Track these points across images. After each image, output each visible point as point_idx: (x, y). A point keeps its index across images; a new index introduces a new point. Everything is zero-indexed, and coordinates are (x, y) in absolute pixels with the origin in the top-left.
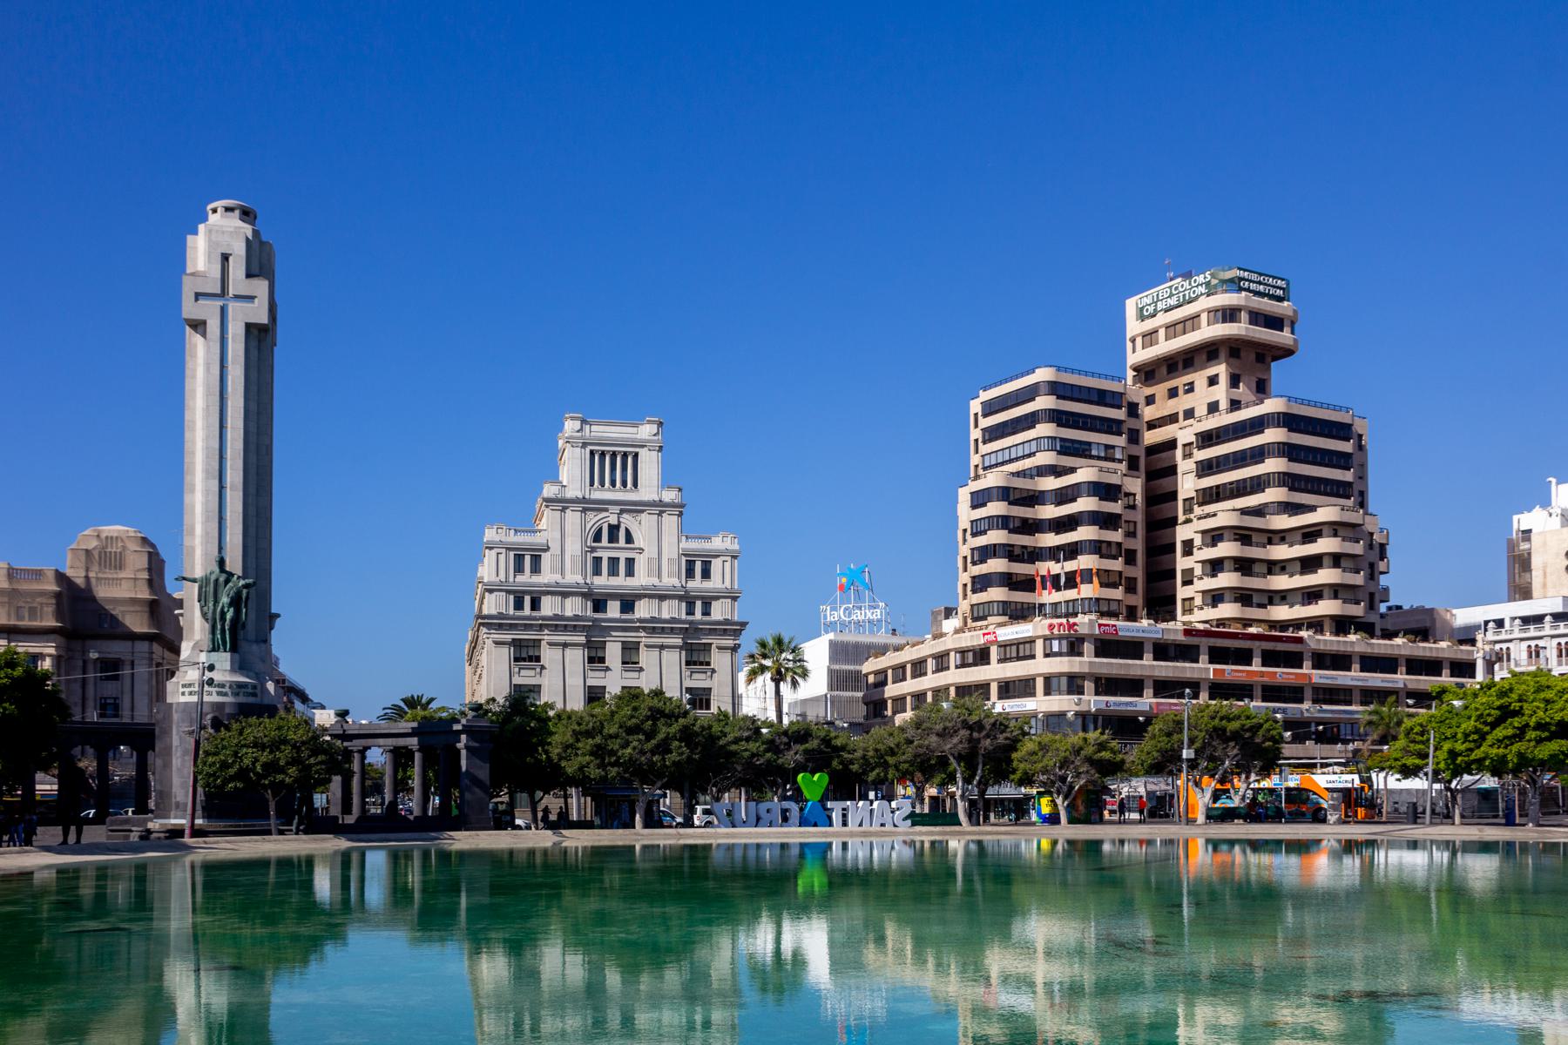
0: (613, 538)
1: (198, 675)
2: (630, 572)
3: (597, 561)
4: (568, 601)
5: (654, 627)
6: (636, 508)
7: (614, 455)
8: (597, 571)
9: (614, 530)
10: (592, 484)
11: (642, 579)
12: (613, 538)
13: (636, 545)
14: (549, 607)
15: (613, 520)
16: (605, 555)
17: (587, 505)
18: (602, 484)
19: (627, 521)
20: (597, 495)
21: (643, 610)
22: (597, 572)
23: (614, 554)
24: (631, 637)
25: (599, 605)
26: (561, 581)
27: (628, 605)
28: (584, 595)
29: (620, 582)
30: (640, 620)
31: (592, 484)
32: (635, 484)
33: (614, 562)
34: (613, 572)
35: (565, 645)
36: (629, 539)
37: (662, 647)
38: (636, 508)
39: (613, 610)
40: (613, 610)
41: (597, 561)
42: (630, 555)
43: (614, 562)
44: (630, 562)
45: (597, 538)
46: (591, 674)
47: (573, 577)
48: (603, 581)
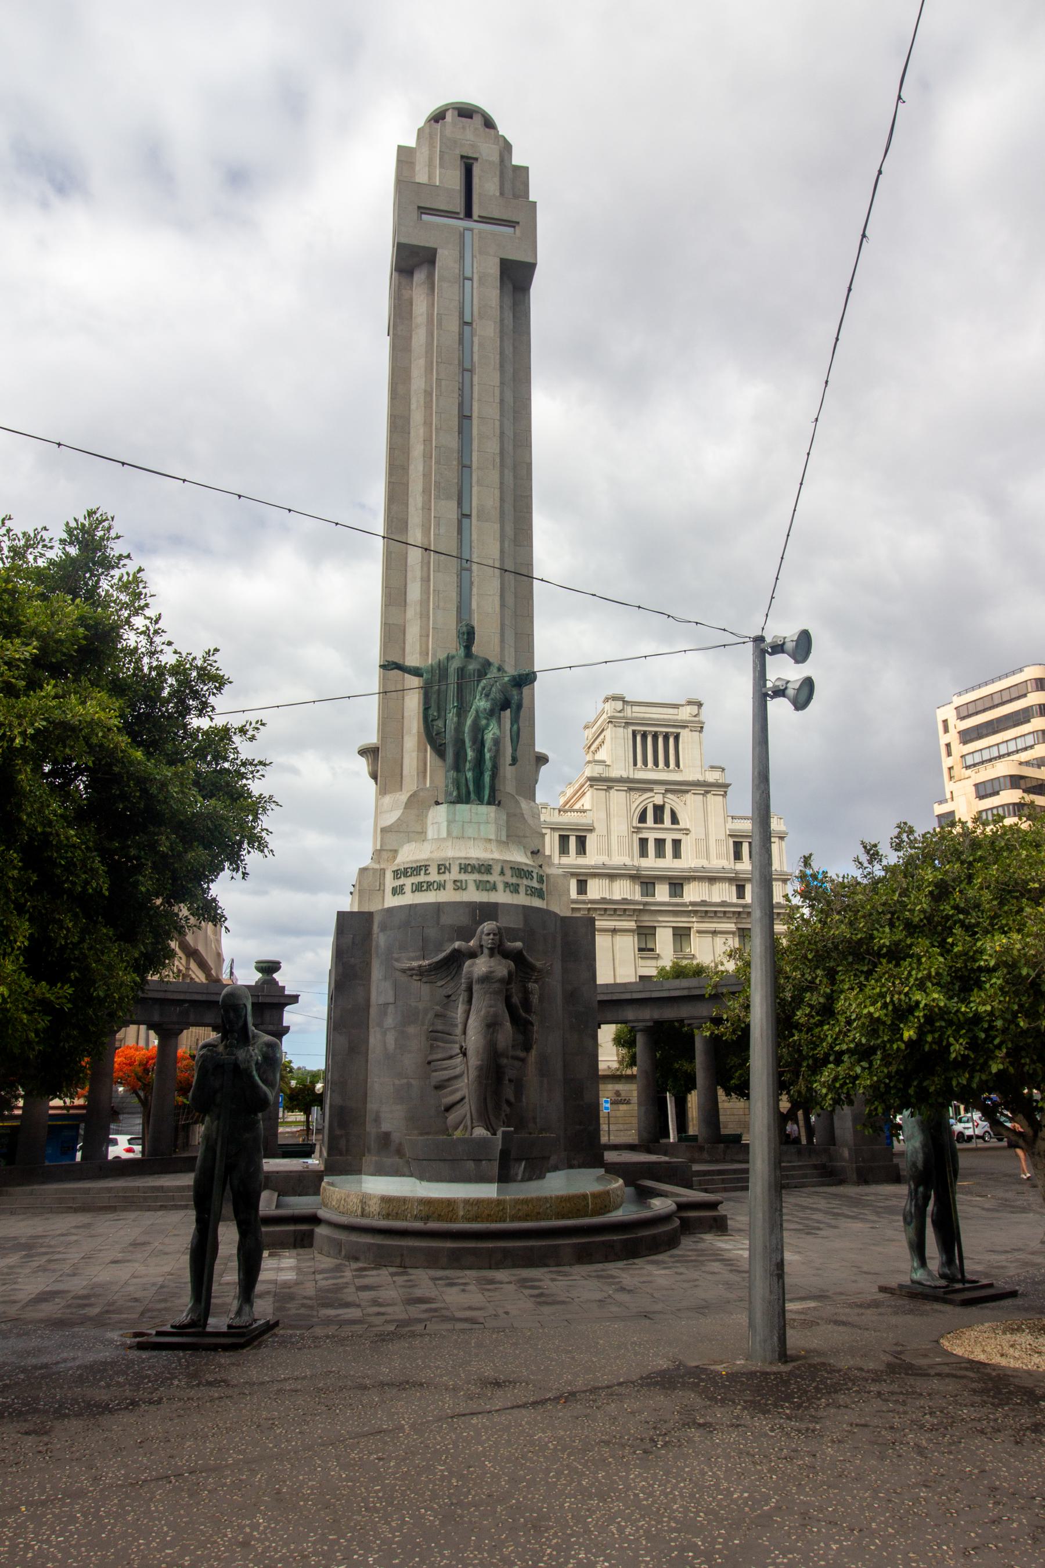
0: (658, 818)
2: (677, 854)
3: (643, 842)
5: (705, 911)
6: (680, 788)
7: (655, 736)
8: (644, 853)
9: (659, 810)
10: (635, 764)
11: (689, 860)
12: (658, 818)
13: (682, 825)
15: (658, 800)
16: (652, 836)
17: (633, 786)
18: (645, 763)
19: (672, 801)
21: (693, 893)
23: (660, 835)
24: (682, 922)
26: (608, 862)
27: (676, 885)
28: (634, 878)
29: (668, 863)
30: (693, 904)
31: (635, 764)
32: (678, 765)
33: (660, 843)
34: (660, 853)
36: (675, 820)
37: (715, 933)
38: (680, 788)
39: (662, 893)
40: (662, 893)
41: (643, 842)
42: (677, 836)
44: (677, 843)
45: (643, 818)
46: (641, 962)
48: (651, 863)
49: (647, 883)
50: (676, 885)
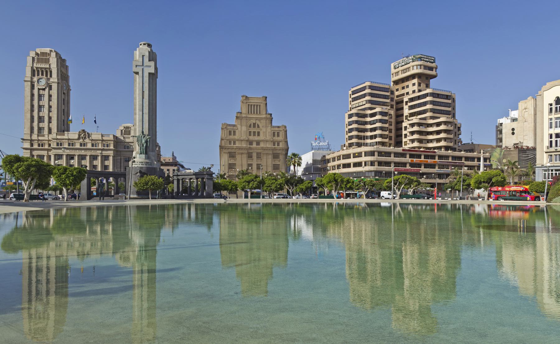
0: (254, 126)
1: (138, 159)
2: (259, 135)
3: (250, 132)
4: (243, 142)
7: (254, 105)
8: (250, 135)
9: (254, 124)
11: (262, 137)
14: (238, 144)
19: (258, 122)
20: (249, 116)
21: (262, 145)
22: (250, 135)
24: (259, 151)
25: (251, 143)
27: (258, 143)
29: (256, 138)
35: (242, 154)
39: (254, 145)
40: (254, 145)
41: (250, 132)
43: (254, 132)
44: (259, 133)
47: (244, 137)
48: (252, 138)
49: (251, 143)
50: (258, 143)
